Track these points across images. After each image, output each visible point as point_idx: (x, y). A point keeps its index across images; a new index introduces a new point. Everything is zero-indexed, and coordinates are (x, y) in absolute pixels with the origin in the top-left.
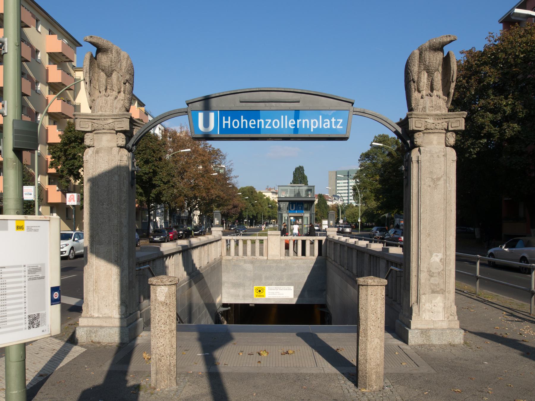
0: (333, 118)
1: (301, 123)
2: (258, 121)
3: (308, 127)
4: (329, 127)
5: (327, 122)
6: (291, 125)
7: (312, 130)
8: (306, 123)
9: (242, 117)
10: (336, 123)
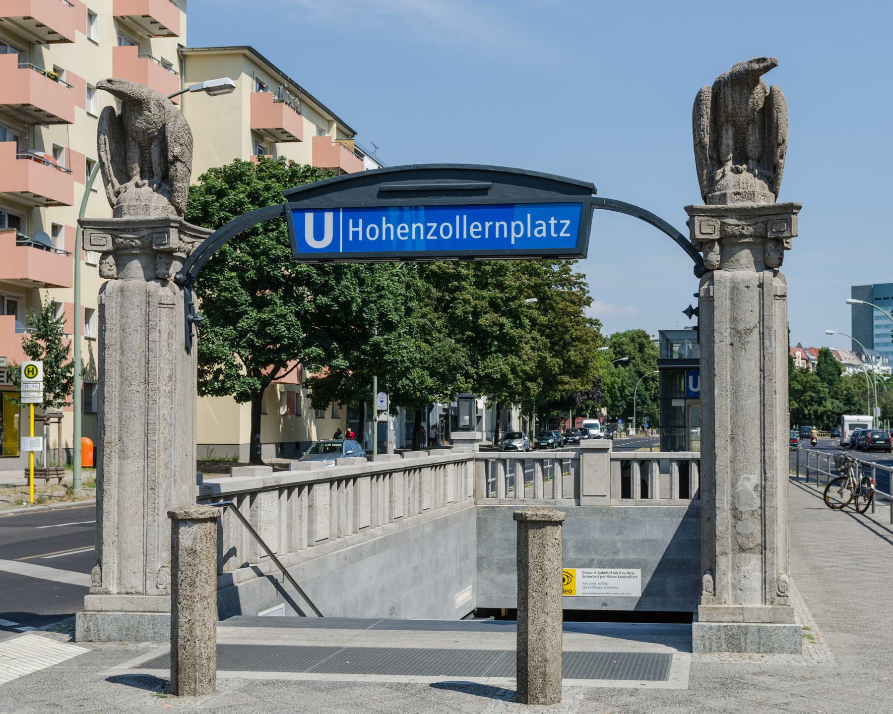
0: (553, 218)
1: (492, 229)
2: (414, 226)
3: (506, 236)
4: (544, 234)
5: (541, 225)
6: (474, 232)
7: (513, 242)
8: (501, 227)
9: (384, 219)
10: (558, 228)
